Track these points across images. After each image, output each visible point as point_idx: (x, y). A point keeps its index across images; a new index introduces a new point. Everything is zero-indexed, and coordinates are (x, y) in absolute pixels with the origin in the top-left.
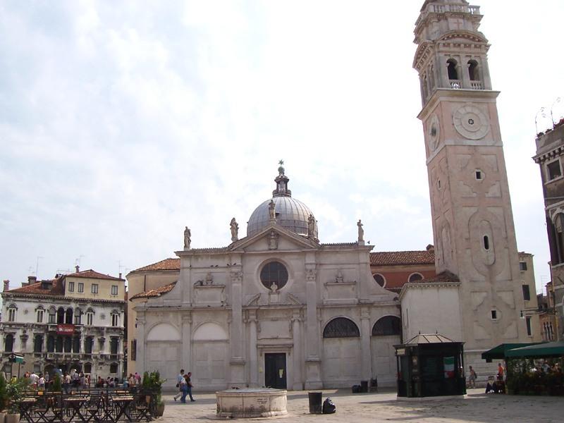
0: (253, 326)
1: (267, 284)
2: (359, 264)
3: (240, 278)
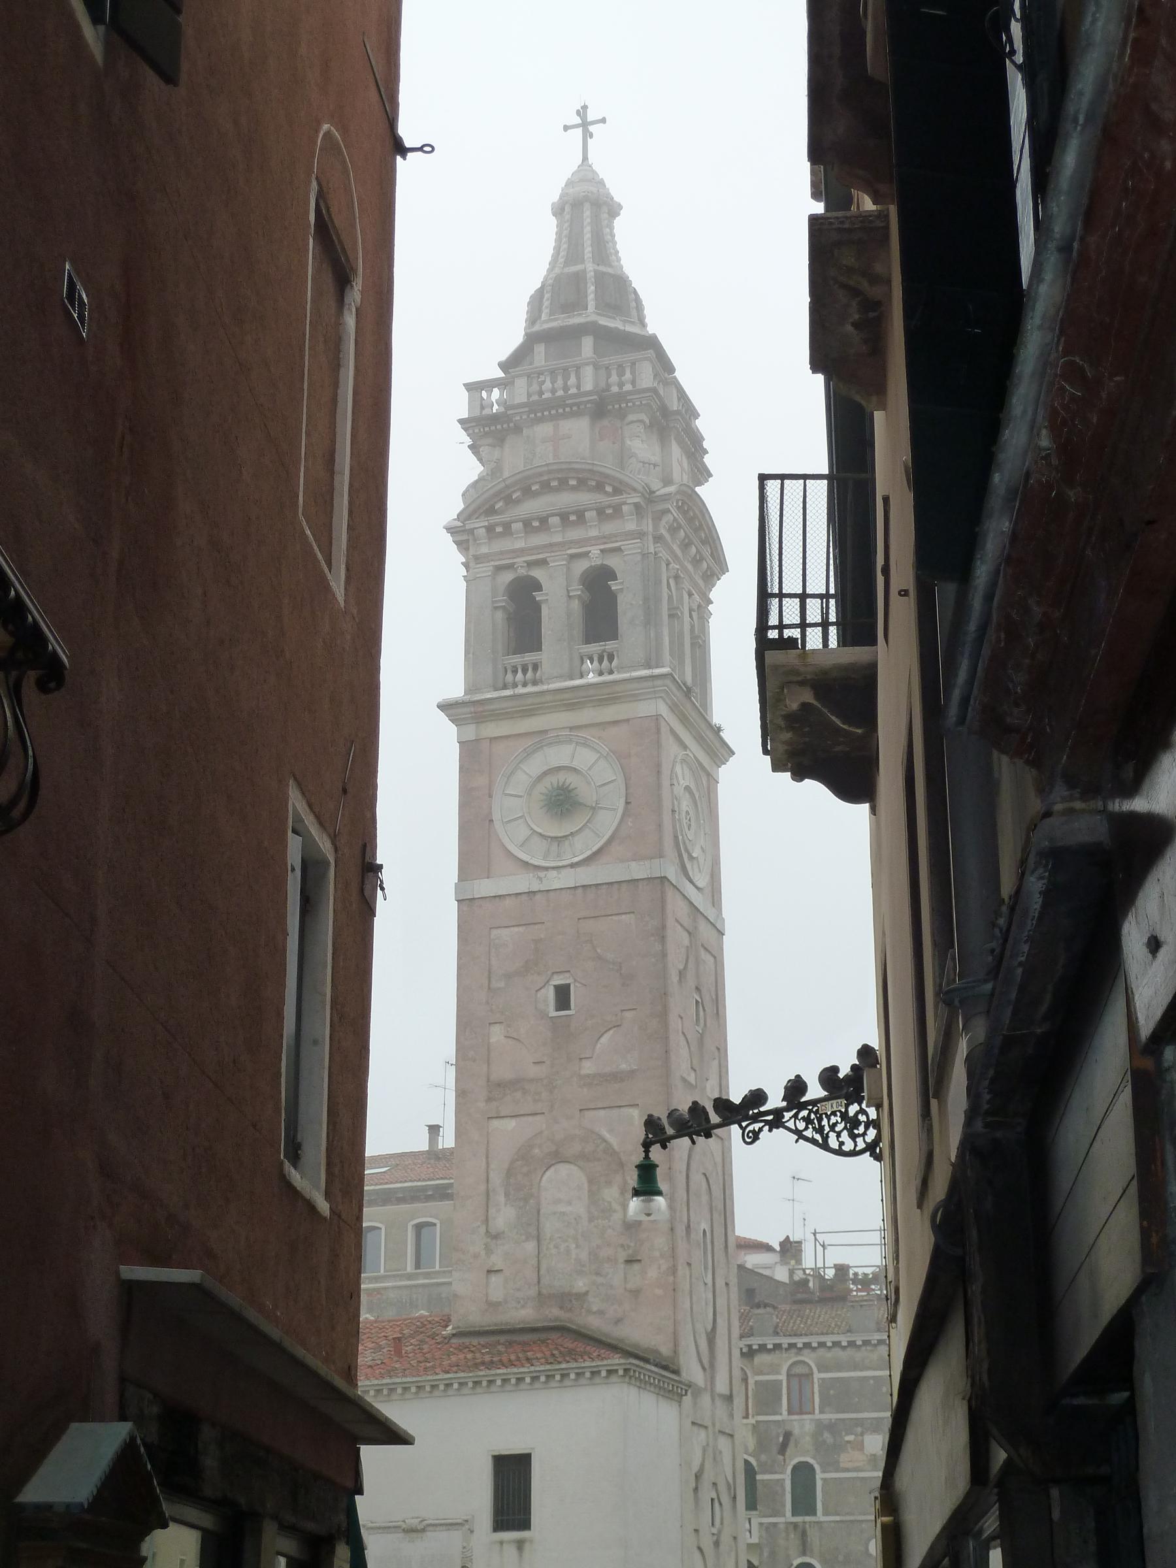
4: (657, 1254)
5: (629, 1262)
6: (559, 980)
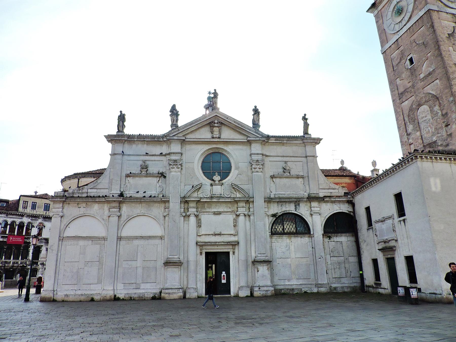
0: (193, 219)
1: (208, 174)
2: (306, 157)
3: (179, 166)
4: (454, 120)
5: (447, 126)
6: (409, 58)
